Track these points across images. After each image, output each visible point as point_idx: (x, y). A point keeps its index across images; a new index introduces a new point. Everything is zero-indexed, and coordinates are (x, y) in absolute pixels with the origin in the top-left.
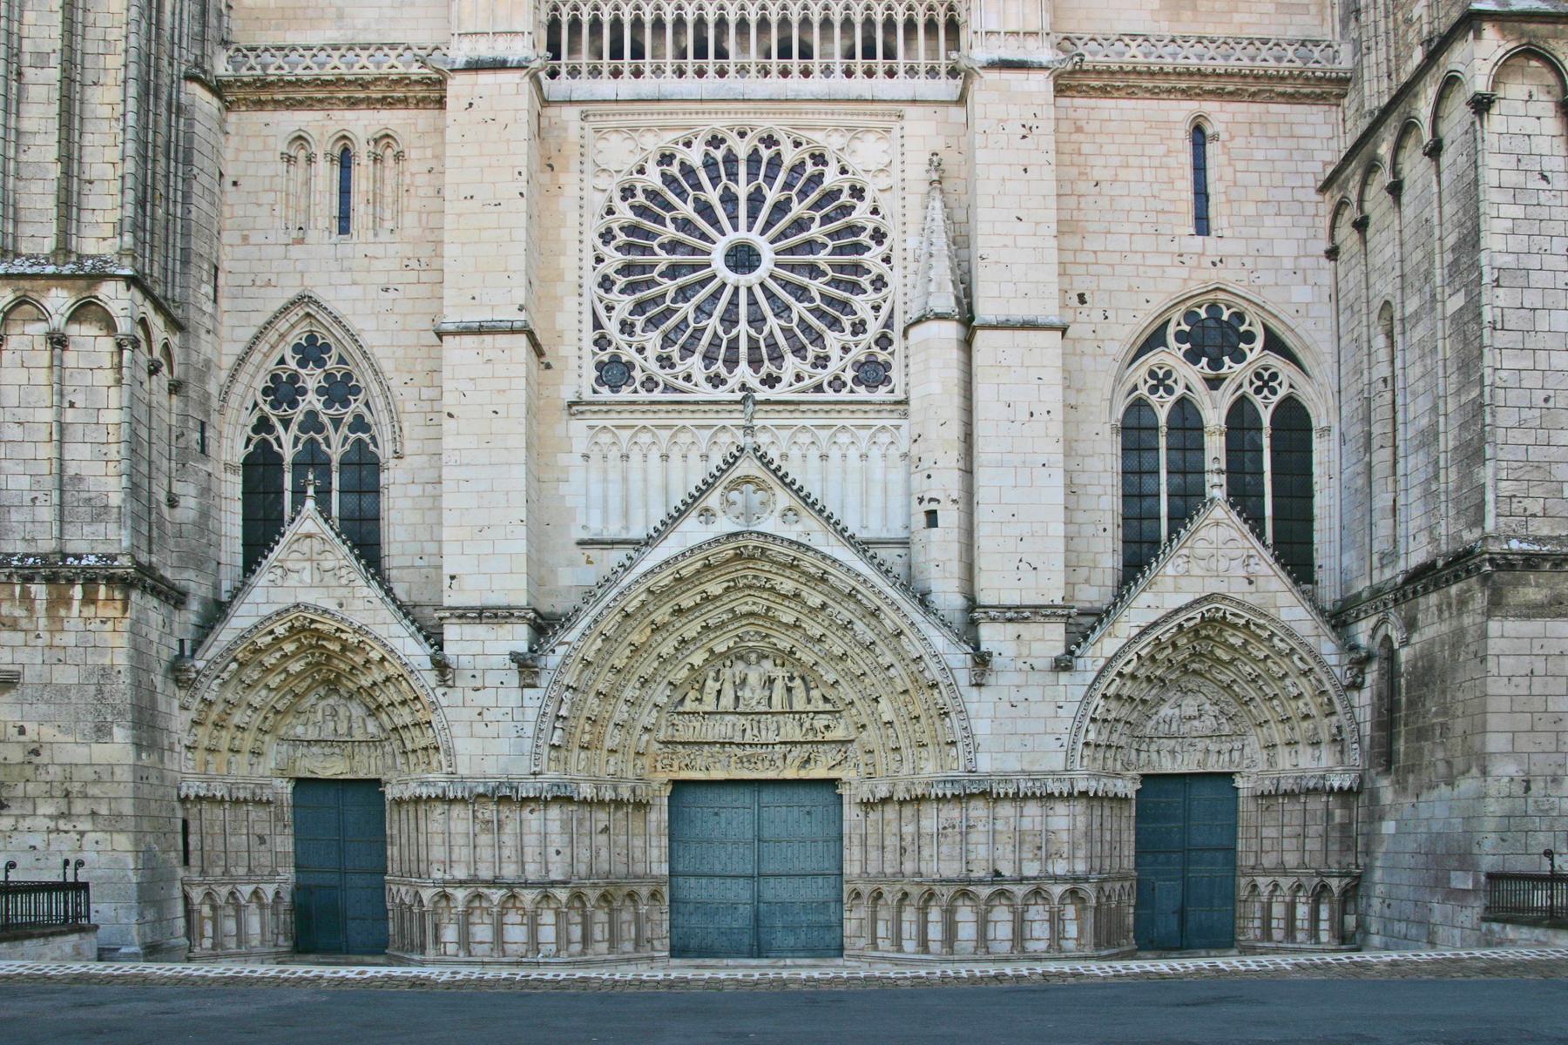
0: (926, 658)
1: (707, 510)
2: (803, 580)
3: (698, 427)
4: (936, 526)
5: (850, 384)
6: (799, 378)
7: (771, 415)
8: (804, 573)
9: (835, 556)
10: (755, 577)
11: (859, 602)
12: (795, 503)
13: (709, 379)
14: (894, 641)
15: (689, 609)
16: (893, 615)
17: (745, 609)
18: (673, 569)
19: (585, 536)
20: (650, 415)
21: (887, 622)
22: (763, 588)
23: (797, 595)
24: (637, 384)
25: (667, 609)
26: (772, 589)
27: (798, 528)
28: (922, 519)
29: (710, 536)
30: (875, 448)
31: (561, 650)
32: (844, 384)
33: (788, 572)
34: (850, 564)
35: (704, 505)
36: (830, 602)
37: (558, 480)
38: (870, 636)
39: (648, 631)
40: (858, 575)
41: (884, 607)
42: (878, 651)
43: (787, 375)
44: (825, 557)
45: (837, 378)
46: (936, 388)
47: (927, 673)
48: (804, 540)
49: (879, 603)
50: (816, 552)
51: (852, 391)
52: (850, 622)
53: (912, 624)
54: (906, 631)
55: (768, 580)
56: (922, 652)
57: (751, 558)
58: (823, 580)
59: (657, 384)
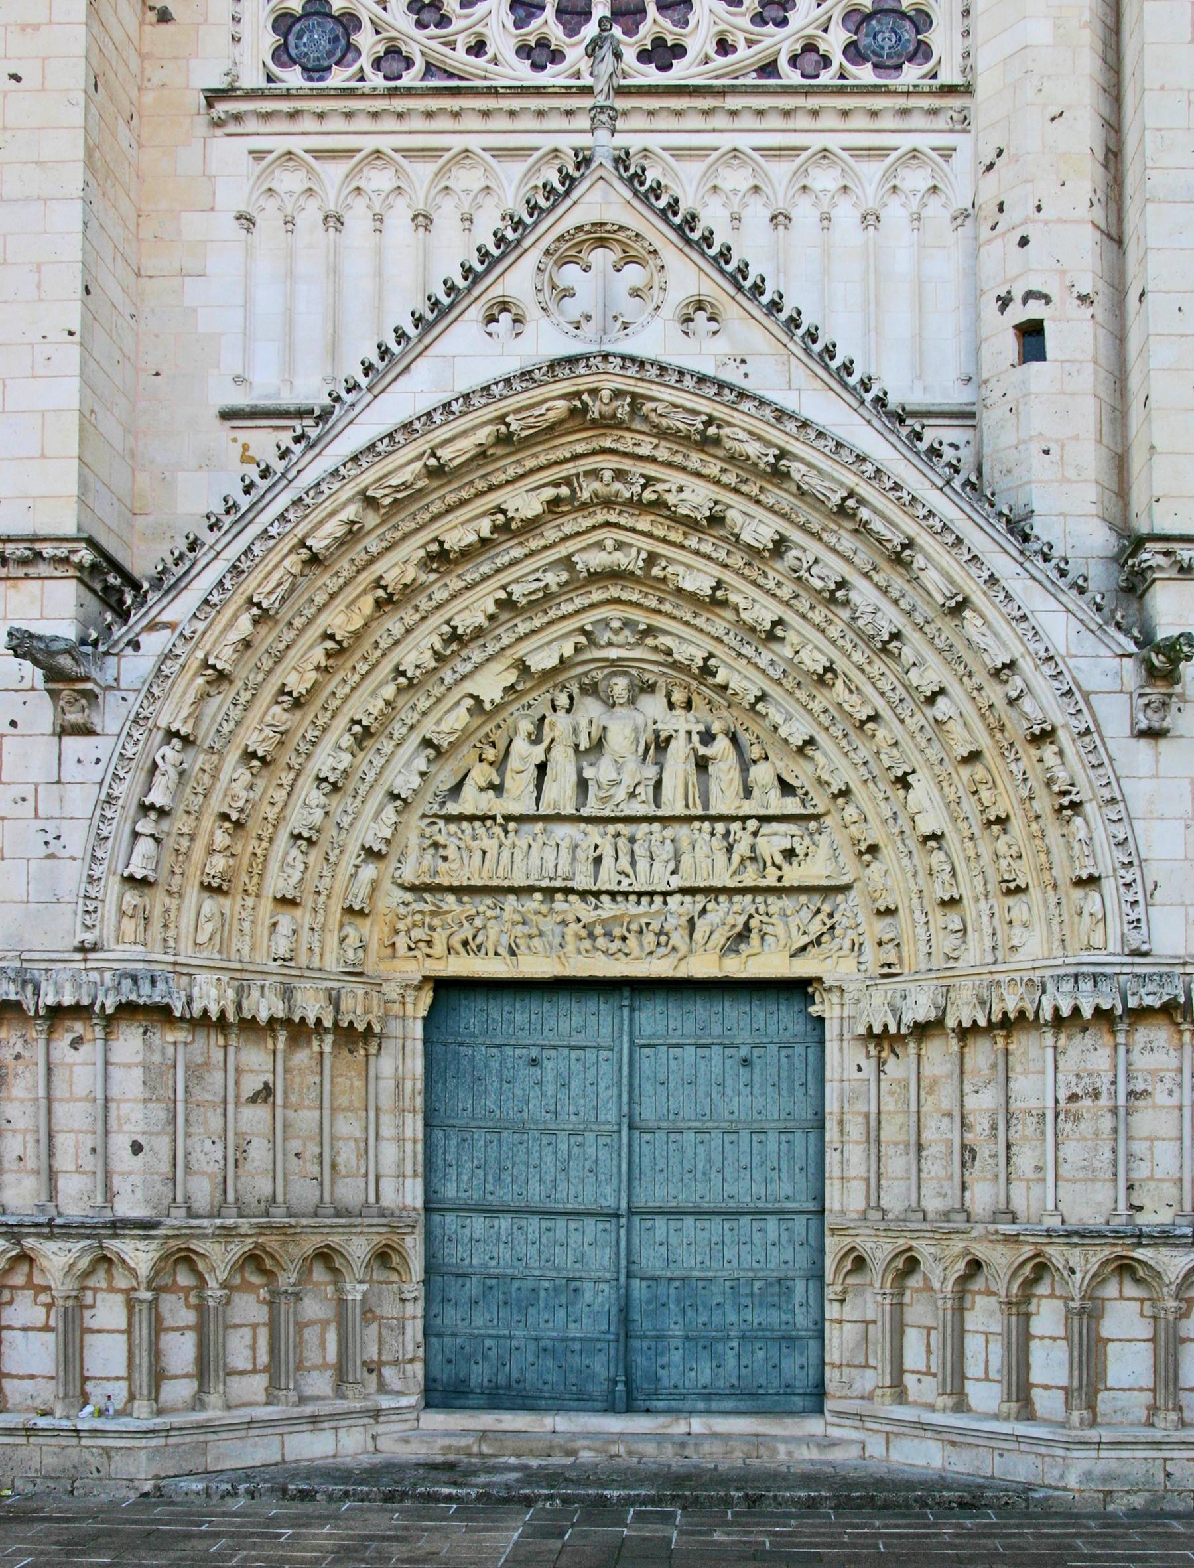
0: (1026, 664)
1: (505, 306)
2: (730, 479)
3: (500, 153)
4: (1041, 357)
5: (838, 58)
6: (724, 47)
7: (661, 123)
8: (732, 458)
9: (806, 413)
10: (619, 475)
11: (863, 530)
12: (713, 287)
13: (524, 51)
14: (947, 626)
15: (466, 554)
16: (945, 559)
17: (597, 560)
18: (422, 445)
19: (239, 399)
20: (390, 124)
21: (931, 578)
22: (636, 504)
23: (716, 520)
24: (365, 61)
25: (413, 549)
26: (659, 504)
27: (720, 346)
28: (1010, 344)
29: (512, 366)
30: (895, 202)
31: (154, 643)
32: (826, 61)
33: (695, 460)
34: (842, 434)
35: (496, 291)
36: (796, 535)
37: (182, 273)
38: (889, 619)
39: (367, 604)
40: (861, 459)
41: (924, 539)
42: (908, 654)
43: (699, 41)
44: (781, 414)
45: (810, 48)
46: (1040, 32)
47: (1027, 704)
48: (731, 375)
49: (912, 528)
50: (762, 403)
51: (842, 77)
52: (842, 584)
53: (993, 580)
54: (978, 598)
55: (649, 481)
56: (1017, 650)
57: (609, 423)
58: (778, 475)
59: (409, 63)
